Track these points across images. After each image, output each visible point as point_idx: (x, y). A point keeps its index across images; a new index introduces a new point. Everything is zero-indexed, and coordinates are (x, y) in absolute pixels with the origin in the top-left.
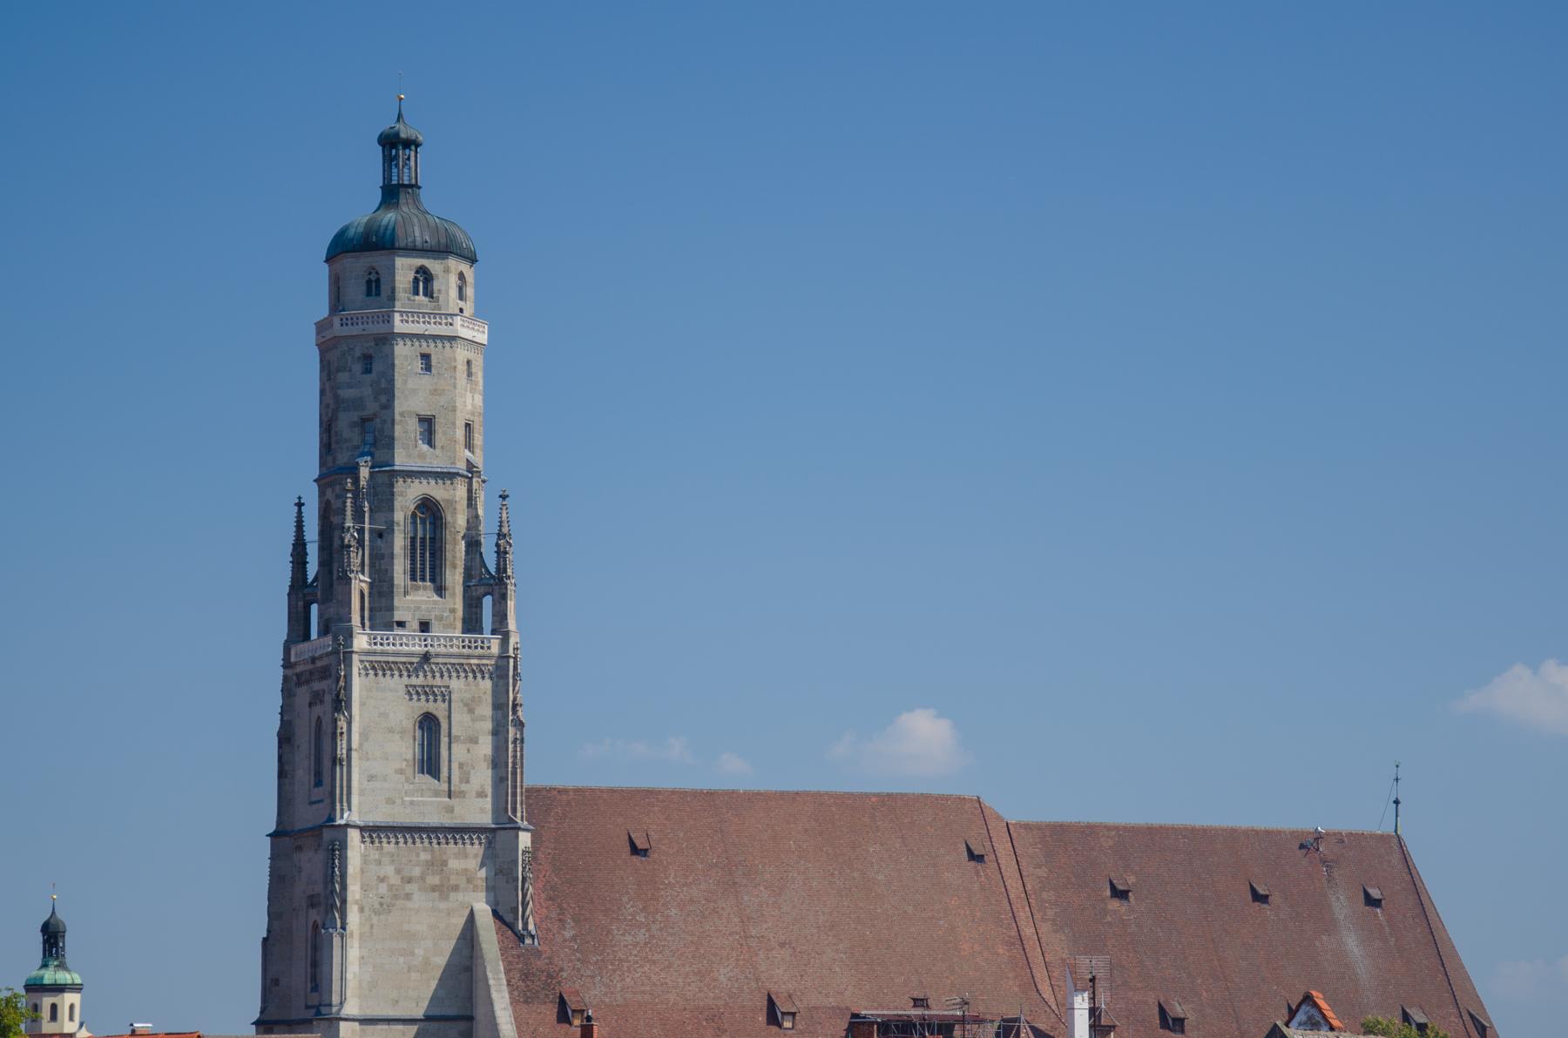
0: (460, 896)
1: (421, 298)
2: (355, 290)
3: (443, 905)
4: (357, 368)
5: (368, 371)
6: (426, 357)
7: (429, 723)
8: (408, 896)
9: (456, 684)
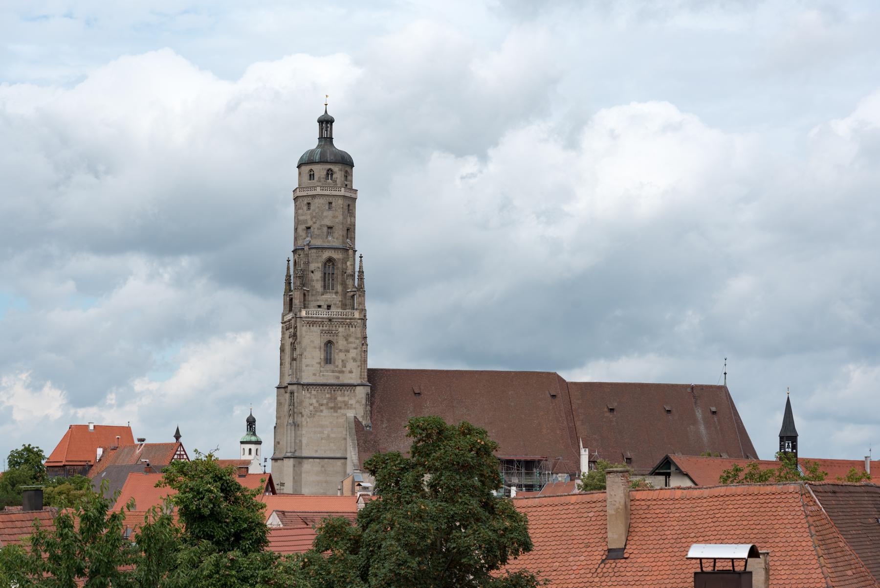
0: (342, 411)
1: (330, 181)
2: (306, 177)
3: (335, 414)
4: (305, 208)
5: (309, 209)
6: (330, 203)
7: (329, 343)
9: (341, 329)
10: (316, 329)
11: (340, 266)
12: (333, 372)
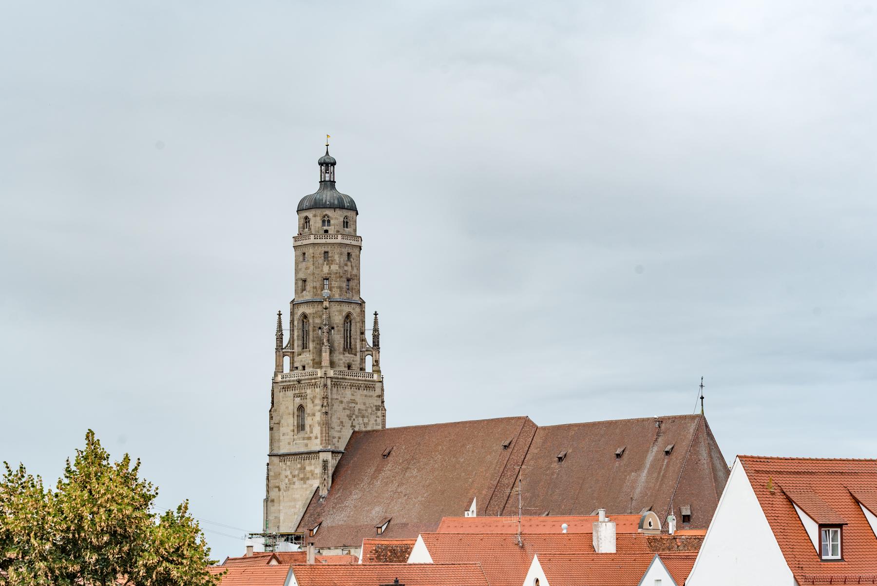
3: (305, 486)
7: (301, 408)
8: (294, 483)
9: (309, 391)
10: (290, 393)
11: (311, 321)
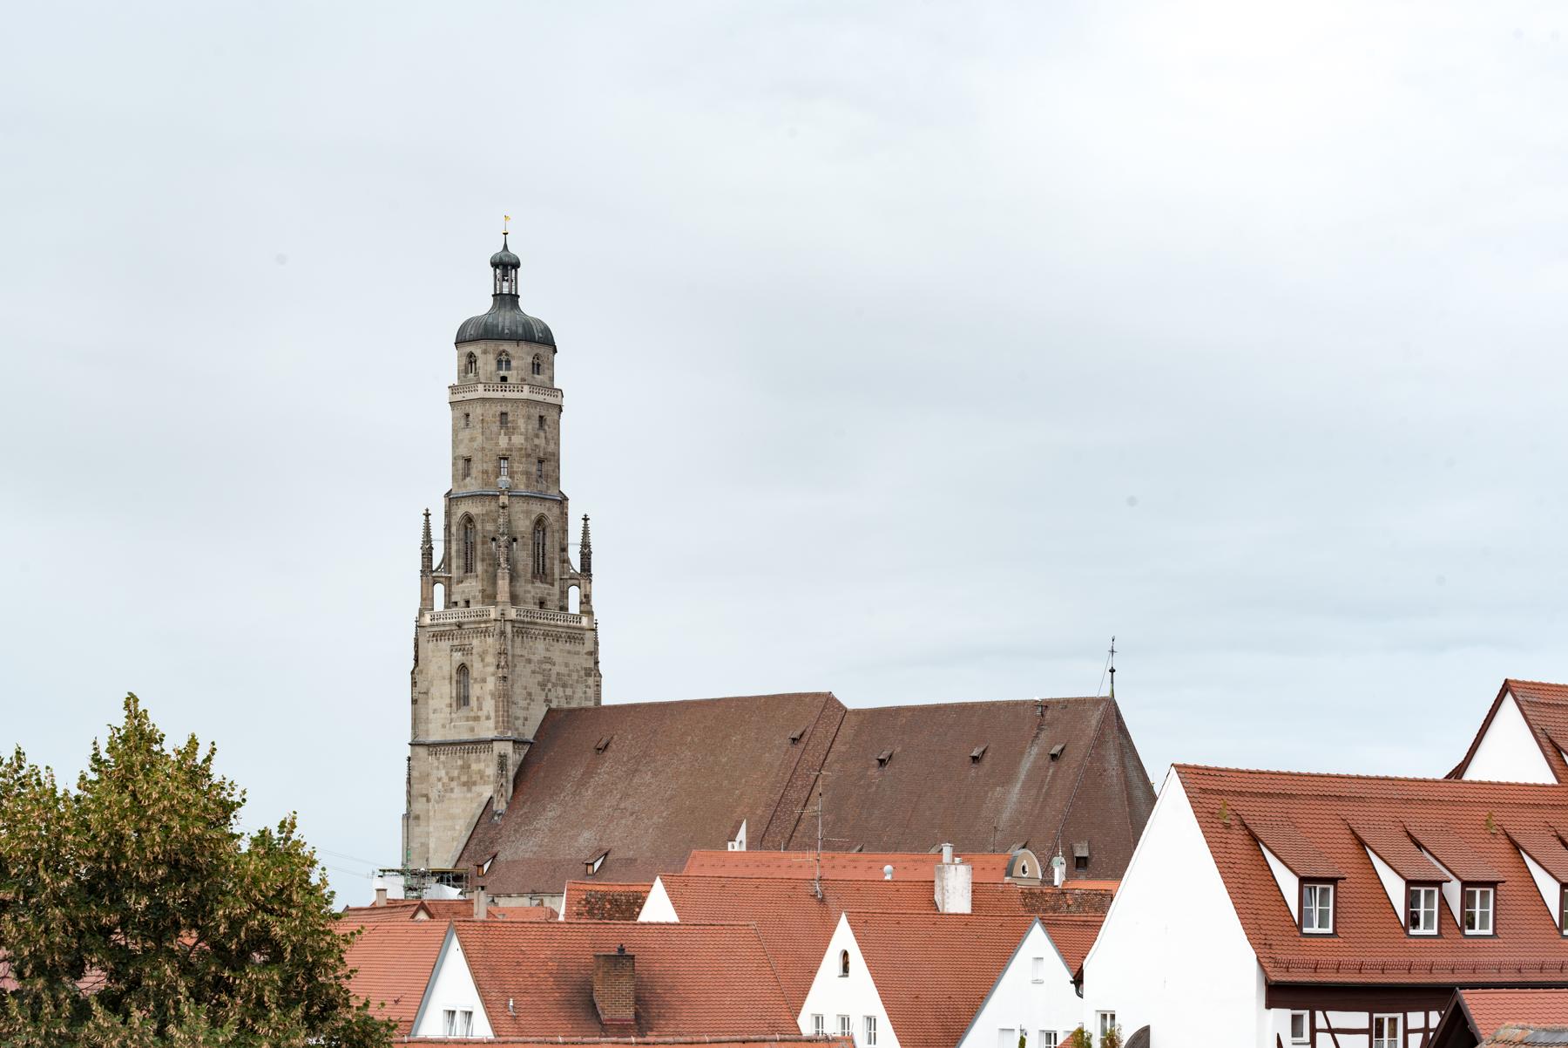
7: (463, 669)
8: (452, 790)
9: (475, 642)
10: (445, 645)
11: (479, 527)
12: (468, 719)
